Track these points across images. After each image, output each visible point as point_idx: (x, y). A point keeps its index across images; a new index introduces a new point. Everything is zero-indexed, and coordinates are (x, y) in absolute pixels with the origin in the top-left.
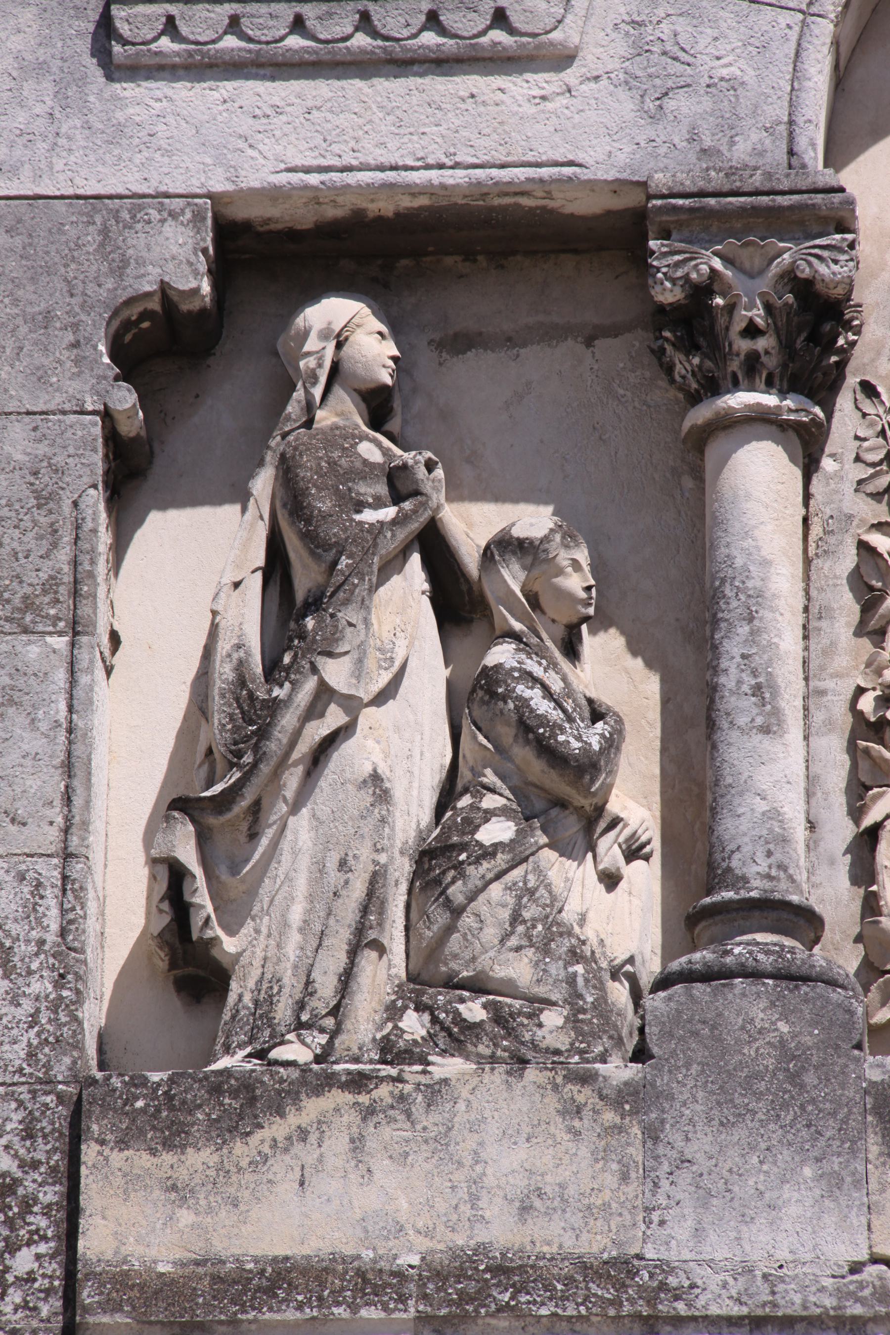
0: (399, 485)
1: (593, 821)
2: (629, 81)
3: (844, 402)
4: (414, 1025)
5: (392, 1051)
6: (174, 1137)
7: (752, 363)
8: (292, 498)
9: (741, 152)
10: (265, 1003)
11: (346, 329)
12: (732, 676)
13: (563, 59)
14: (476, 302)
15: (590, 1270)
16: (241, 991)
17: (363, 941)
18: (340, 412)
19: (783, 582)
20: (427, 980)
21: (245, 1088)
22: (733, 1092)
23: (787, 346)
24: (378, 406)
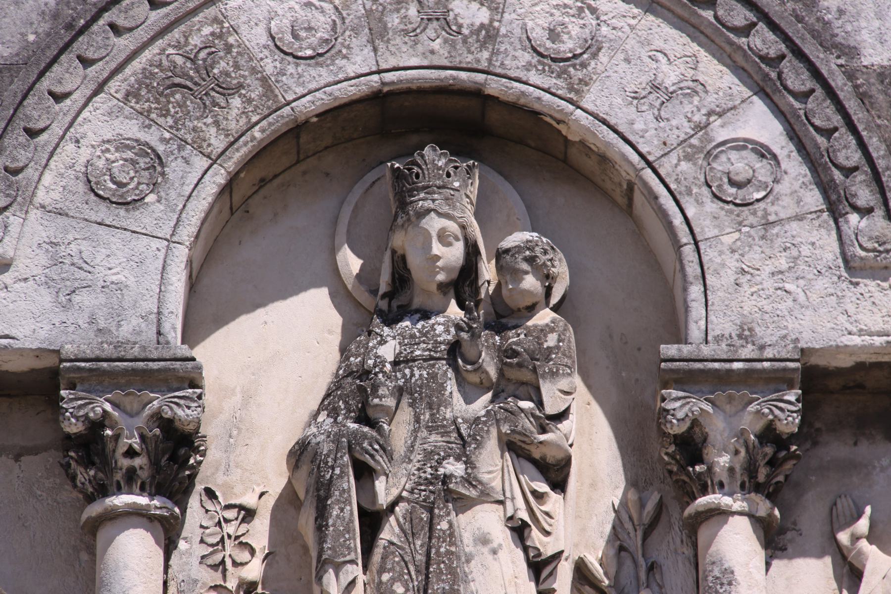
2: (49, 282)
3: (194, 502)
7: (131, 475)
9: (125, 331)
23: (155, 463)
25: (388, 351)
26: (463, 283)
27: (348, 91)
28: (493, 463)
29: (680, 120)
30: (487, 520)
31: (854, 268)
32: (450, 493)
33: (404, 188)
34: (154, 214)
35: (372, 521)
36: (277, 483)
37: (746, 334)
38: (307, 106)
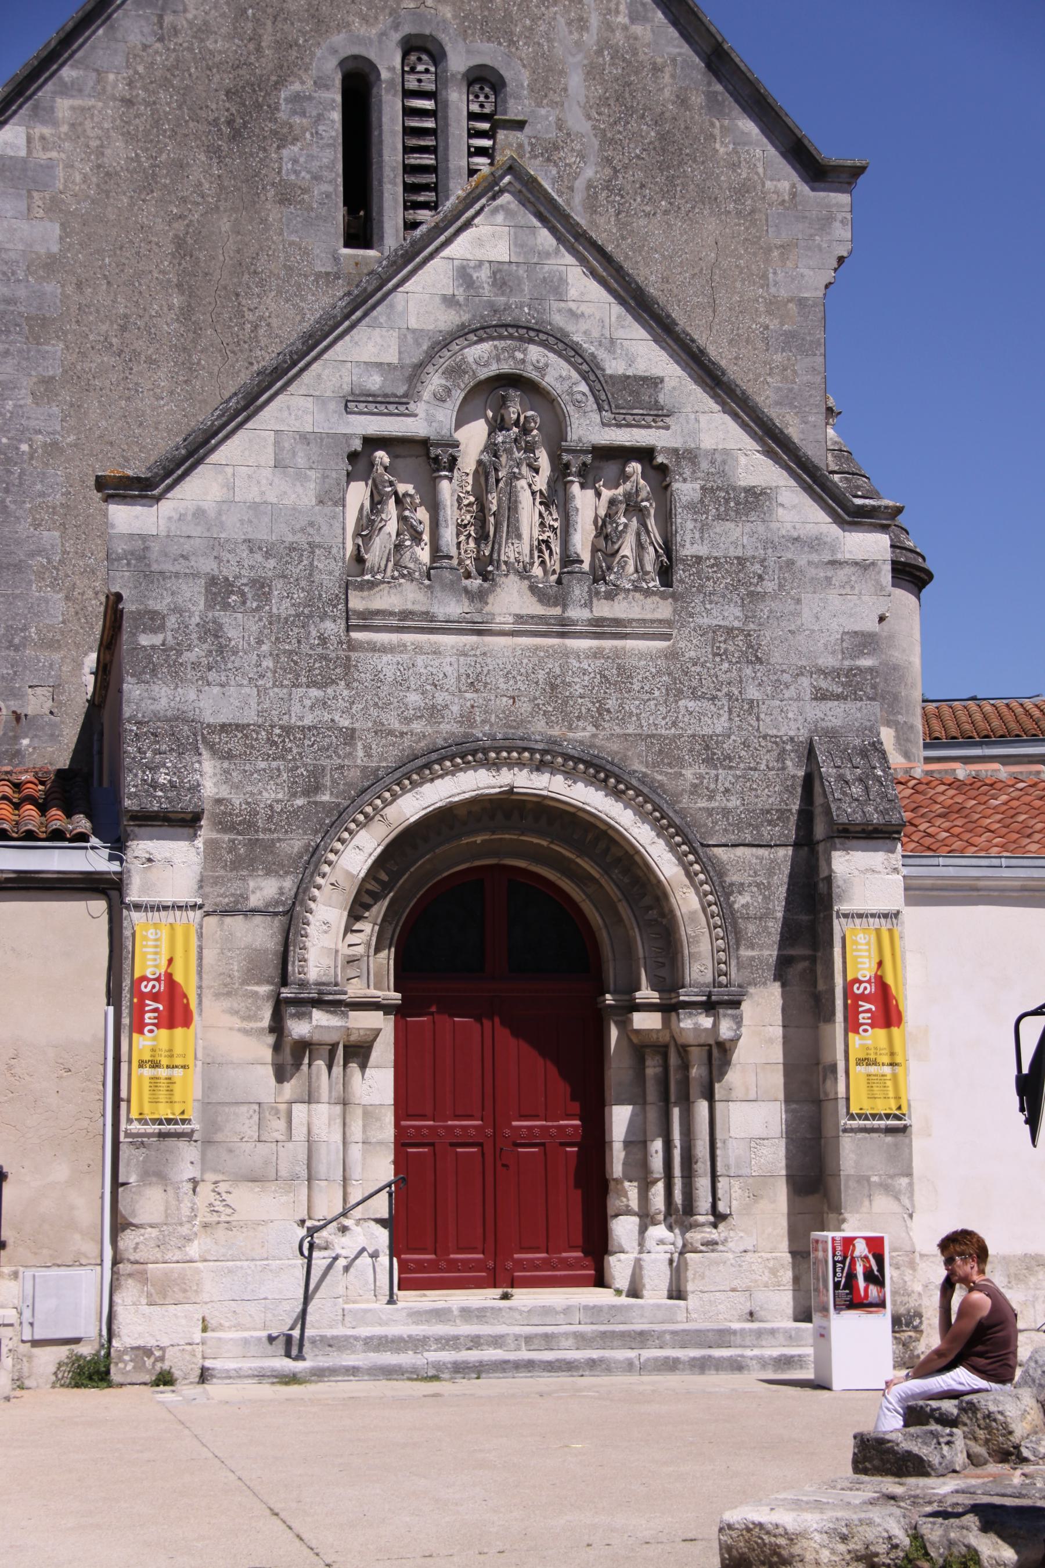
0: (391, 484)
1: (421, 540)
4: (396, 574)
5: (393, 577)
6: (362, 590)
10: (373, 568)
11: (381, 456)
12: (441, 518)
13: (416, 416)
14: (399, 450)
15: (423, 613)
16: (368, 564)
17: (388, 560)
18: (381, 470)
19: (448, 503)
20: (396, 564)
21: (372, 582)
22: (444, 586)
24: (386, 468)
25: (500, 439)
26: (517, 423)
27: (492, 374)
28: (525, 470)
29: (566, 387)
30: (522, 483)
31: (604, 424)
32: (514, 477)
34: (449, 404)
36: (473, 467)
37: (580, 440)
38: (482, 377)
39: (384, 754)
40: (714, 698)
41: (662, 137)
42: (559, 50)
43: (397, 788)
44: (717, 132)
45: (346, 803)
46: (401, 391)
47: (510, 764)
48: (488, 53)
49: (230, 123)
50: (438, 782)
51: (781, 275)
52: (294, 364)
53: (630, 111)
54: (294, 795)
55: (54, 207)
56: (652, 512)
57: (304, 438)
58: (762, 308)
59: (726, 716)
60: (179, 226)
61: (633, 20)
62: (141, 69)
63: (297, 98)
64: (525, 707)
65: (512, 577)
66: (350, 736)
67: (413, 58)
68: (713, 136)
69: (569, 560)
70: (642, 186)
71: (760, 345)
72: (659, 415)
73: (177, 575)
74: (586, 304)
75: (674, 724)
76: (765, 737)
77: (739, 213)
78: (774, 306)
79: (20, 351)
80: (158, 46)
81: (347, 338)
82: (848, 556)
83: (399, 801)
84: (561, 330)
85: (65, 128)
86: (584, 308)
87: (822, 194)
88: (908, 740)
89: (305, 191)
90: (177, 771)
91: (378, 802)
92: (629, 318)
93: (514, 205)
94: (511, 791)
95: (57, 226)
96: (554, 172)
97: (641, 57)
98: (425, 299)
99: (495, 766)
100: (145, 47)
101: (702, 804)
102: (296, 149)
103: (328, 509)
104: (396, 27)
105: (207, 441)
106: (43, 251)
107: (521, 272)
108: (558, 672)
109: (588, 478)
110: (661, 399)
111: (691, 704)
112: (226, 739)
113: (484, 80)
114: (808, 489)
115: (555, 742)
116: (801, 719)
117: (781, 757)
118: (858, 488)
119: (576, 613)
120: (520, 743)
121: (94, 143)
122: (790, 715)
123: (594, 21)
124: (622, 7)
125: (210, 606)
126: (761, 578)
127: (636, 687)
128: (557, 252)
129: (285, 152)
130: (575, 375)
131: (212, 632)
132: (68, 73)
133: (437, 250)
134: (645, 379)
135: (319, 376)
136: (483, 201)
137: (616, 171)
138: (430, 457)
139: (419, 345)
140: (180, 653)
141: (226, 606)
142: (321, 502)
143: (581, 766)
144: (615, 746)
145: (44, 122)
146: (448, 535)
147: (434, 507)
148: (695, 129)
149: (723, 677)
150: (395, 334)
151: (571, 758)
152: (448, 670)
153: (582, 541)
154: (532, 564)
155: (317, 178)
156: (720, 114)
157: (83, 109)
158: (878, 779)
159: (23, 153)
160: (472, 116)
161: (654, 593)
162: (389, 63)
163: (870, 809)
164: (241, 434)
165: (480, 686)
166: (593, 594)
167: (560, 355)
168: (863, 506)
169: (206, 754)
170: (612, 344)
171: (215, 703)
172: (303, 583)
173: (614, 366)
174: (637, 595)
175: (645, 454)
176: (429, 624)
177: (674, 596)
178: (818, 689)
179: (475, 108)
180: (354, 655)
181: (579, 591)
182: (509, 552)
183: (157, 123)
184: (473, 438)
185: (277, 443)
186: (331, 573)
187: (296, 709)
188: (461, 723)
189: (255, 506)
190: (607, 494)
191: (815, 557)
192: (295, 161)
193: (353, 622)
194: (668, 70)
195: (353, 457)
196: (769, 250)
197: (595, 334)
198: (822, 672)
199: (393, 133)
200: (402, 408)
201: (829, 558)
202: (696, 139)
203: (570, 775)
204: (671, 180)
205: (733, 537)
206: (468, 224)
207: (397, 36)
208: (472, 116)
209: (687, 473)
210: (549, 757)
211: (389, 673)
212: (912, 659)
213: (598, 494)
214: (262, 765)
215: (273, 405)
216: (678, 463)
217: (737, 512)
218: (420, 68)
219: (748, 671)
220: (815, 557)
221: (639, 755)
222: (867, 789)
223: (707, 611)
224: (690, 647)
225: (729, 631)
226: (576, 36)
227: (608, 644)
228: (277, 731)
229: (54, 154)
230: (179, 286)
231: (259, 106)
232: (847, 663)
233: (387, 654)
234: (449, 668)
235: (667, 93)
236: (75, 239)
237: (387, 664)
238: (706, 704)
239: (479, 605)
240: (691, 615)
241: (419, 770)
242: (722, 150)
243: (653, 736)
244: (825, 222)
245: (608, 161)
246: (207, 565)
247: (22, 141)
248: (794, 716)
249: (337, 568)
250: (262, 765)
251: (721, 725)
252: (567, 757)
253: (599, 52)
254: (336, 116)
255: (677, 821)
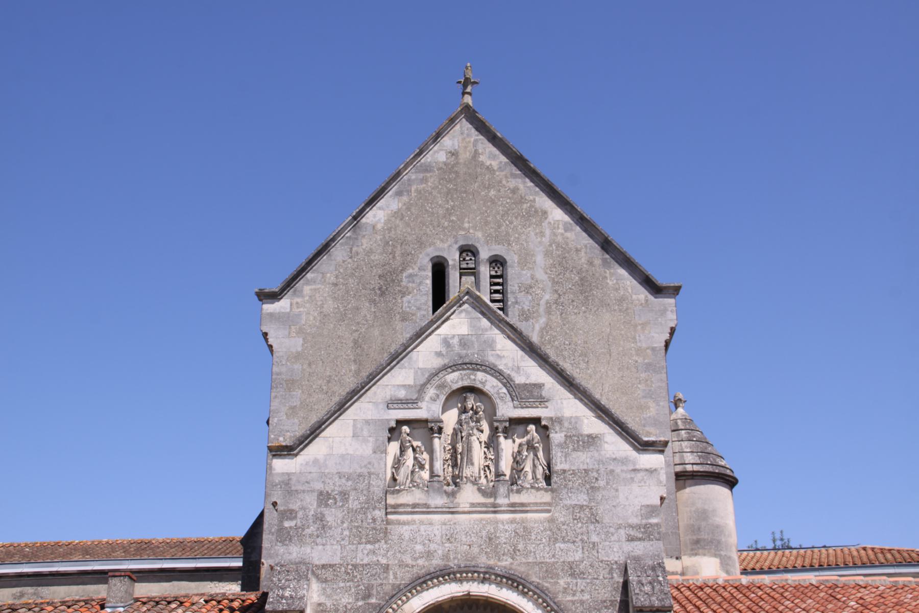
8: (402, 443)
11: (405, 429)
14: (415, 425)
18: (405, 435)
20: (412, 481)
26: (472, 409)
28: (475, 431)
29: (496, 390)
30: (474, 438)
32: (470, 435)
33: (465, 398)
35: (462, 438)
39: (403, 577)
40: (574, 542)
41: (581, 279)
42: (531, 246)
43: (409, 595)
44: (608, 275)
45: (383, 603)
46: (414, 398)
47: (468, 580)
48: (498, 250)
49: (380, 289)
50: (431, 590)
51: (642, 337)
52: (363, 388)
53: (566, 269)
54: (357, 600)
55: (301, 331)
56: (541, 449)
57: (367, 422)
58: (634, 353)
59: (581, 551)
60: (356, 335)
61: (566, 231)
62: (341, 270)
63: (410, 276)
64: (475, 550)
65: (469, 485)
66: (386, 568)
67: (464, 254)
68: (606, 277)
69: (499, 475)
70: (573, 301)
71: (634, 370)
72: (542, 401)
73: (304, 491)
74: (506, 352)
75: (554, 556)
76: (602, 562)
77: (620, 311)
78: (639, 351)
79: (282, 395)
80: (350, 260)
81: (389, 374)
82: (642, 467)
83: (411, 601)
84: (493, 364)
85: (307, 298)
86: (504, 353)
87: (661, 299)
88: (727, 564)
89: (413, 315)
90: (295, 590)
91: (400, 602)
92: (527, 357)
93: (470, 309)
94: (468, 594)
95: (301, 339)
96: (530, 297)
97: (570, 246)
98: (427, 355)
99: (460, 581)
100: (344, 261)
101: (569, 598)
102: (409, 297)
103: (377, 456)
104: (456, 243)
105: (320, 427)
106: (294, 351)
107: (474, 339)
108: (492, 531)
109: (507, 433)
110: (544, 394)
111: (562, 546)
112: (324, 573)
113: (497, 262)
114: (619, 434)
115: (491, 568)
116: (621, 552)
117: (611, 571)
118: (694, 436)
119: (501, 501)
120: (472, 569)
121: (319, 303)
122: (615, 550)
123: (548, 232)
124: (561, 226)
125: (319, 506)
126: (597, 479)
127: (533, 537)
128: (491, 328)
129: (405, 299)
130: (500, 385)
131: (320, 517)
132: (310, 275)
133: (433, 332)
134: (535, 385)
135: (375, 393)
136: (455, 308)
137: (560, 295)
138: (429, 428)
139: (423, 375)
140: (303, 530)
141: (327, 505)
142: (375, 452)
143: (504, 580)
144: (523, 569)
145: (298, 296)
146: (438, 465)
147: (431, 452)
148: (597, 275)
149: (578, 531)
150: (412, 371)
151: (499, 575)
152: (437, 532)
153: (506, 465)
154: (480, 477)
155: (419, 309)
156: (609, 267)
157: (315, 290)
158: (660, 582)
159: (288, 310)
160: (492, 277)
161: (541, 489)
162: (453, 258)
163: (654, 598)
164: (337, 422)
165: (452, 540)
166: (510, 491)
167: (492, 375)
168: (647, 442)
169: (314, 581)
170: (518, 369)
171: (319, 554)
172: (365, 492)
173: (519, 379)
174: (533, 491)
175: (536, 421)
176: (427, 510)
177: (552, 491)
178: (629, 535)
179: (493, 273)
180: (389, 527)
181: (502, 490)
182: (467, 472)
183: (347, 292)
184: (450, 419)
185: (354, 426)
186: (378, 487)
187: (360, 555)
188: (443, 559)
189: (343, 457)
190: (518, 441)
191: (625, 468)
192: (409, 302)
193: (389, 510)
194: (583, 251)
195: (391, 430)
196: (635, 326)
197: (510, 365)
198: (631, 526)
199: (455, 287)
200: (415, 405)
201: (631, 468)
202: (598, 279)
203: (499, 584)
204: (586, 298)
205: (582, 459)
206: (448, 319)
207: (457, 246)
208: (492, 277)
209: (557, 428)
210: (487, 576)
211: (407, 535)
212: (728, 522)
213: (514, 441)
214: (342, 585)
215: (352, 407)
216: (553, 424)
217: (583, 447)
218: (468, 258)
219: (592, 527)
220: (625, 468)
221: (535, 573)
222: (653, 588)
223: (570, 497)
224: (561, 515)
225: (581, 507)
226: (539, 239)
227: (518, 516)
228: (350, 567)
229: (302, 309)
230: (355, 361)
231: (393, 281)
232: (644, 521)
233: (406, 527)
234: (437, 531)
235: (583, 260)
236: (309, 344)
237: (405, 531)
238: (570, 545)
239: (452, 499)
240: (561, 500)
241: (421, 584)
242: (611, 283)
243: (542, 563)
244: (663, 312)
245: (556, 291)
246: (319, 486)
247: (289, 305)
248: (617, 550)
249: (381, 484)
250: (342, 585)
251: (578, 556)
252: (497, 575)
253: (551, 245)
254: (429, 282)
255: (555, 608)
